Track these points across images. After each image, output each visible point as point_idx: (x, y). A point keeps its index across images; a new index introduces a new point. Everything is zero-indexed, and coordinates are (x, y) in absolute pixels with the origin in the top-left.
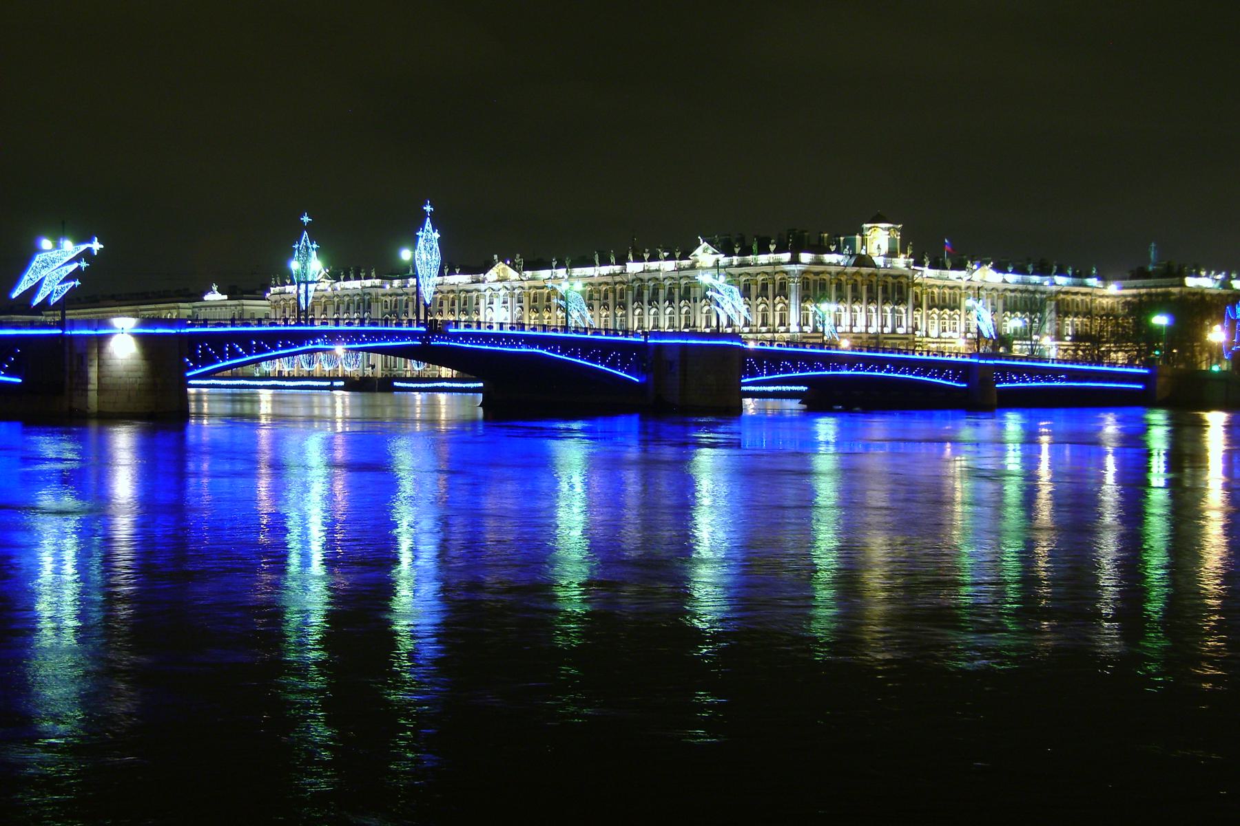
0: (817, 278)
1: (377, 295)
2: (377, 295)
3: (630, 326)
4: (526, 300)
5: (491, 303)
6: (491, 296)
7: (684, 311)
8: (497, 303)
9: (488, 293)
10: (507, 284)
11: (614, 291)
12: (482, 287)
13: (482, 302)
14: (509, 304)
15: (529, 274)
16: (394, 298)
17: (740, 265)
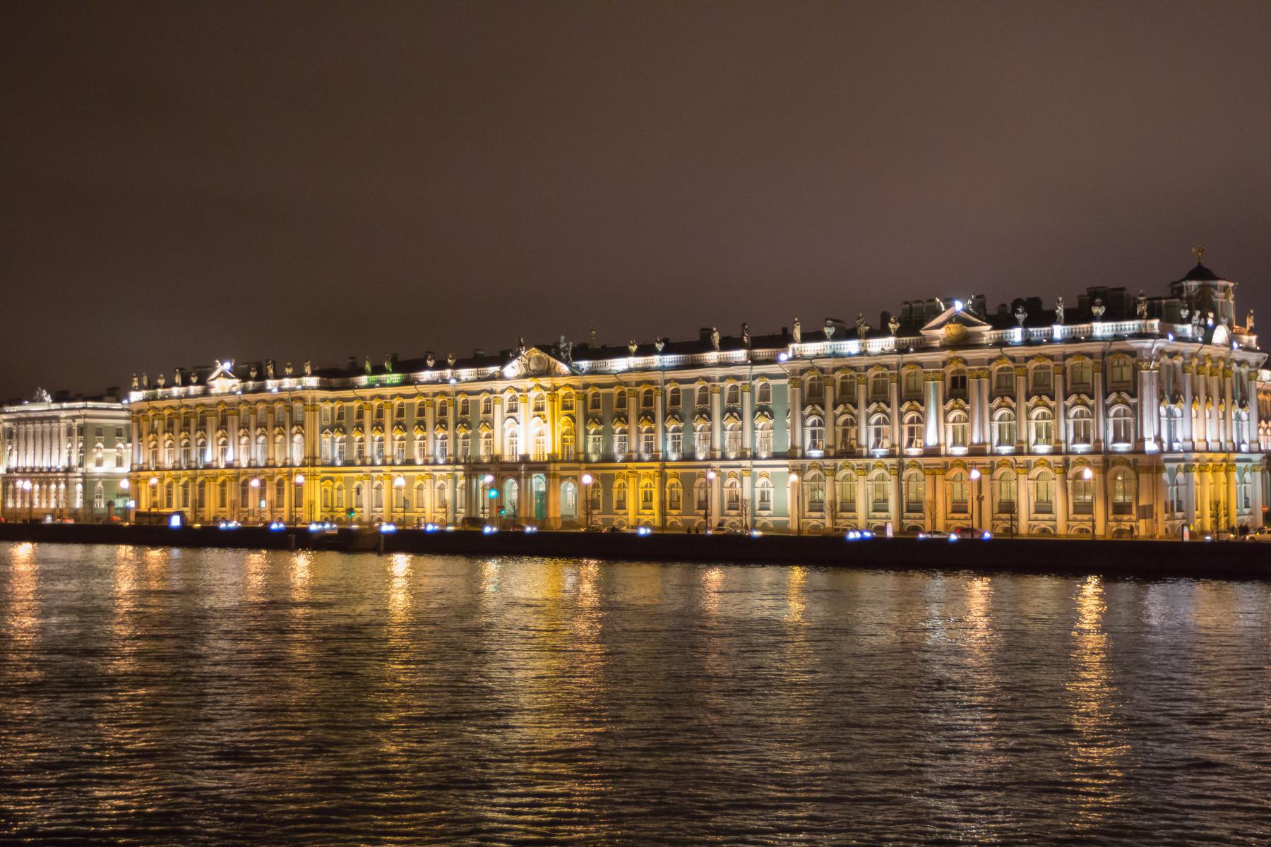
0: (1169, 362)
1: (314, 400)
2: (314, 400)
3: (798, 443)
4: (578, 405)
5: (513, 410)
6: (514, 399)
7: (907, 418)
8: (525, 410)
9: (507, 396)
10: (546, 382)
11: (752, 390)
12: (498, 385)
13: (498, 408)
14: (547, 412)
15: (585, 364)
16: (337, 405)
17: (1066, 341)
